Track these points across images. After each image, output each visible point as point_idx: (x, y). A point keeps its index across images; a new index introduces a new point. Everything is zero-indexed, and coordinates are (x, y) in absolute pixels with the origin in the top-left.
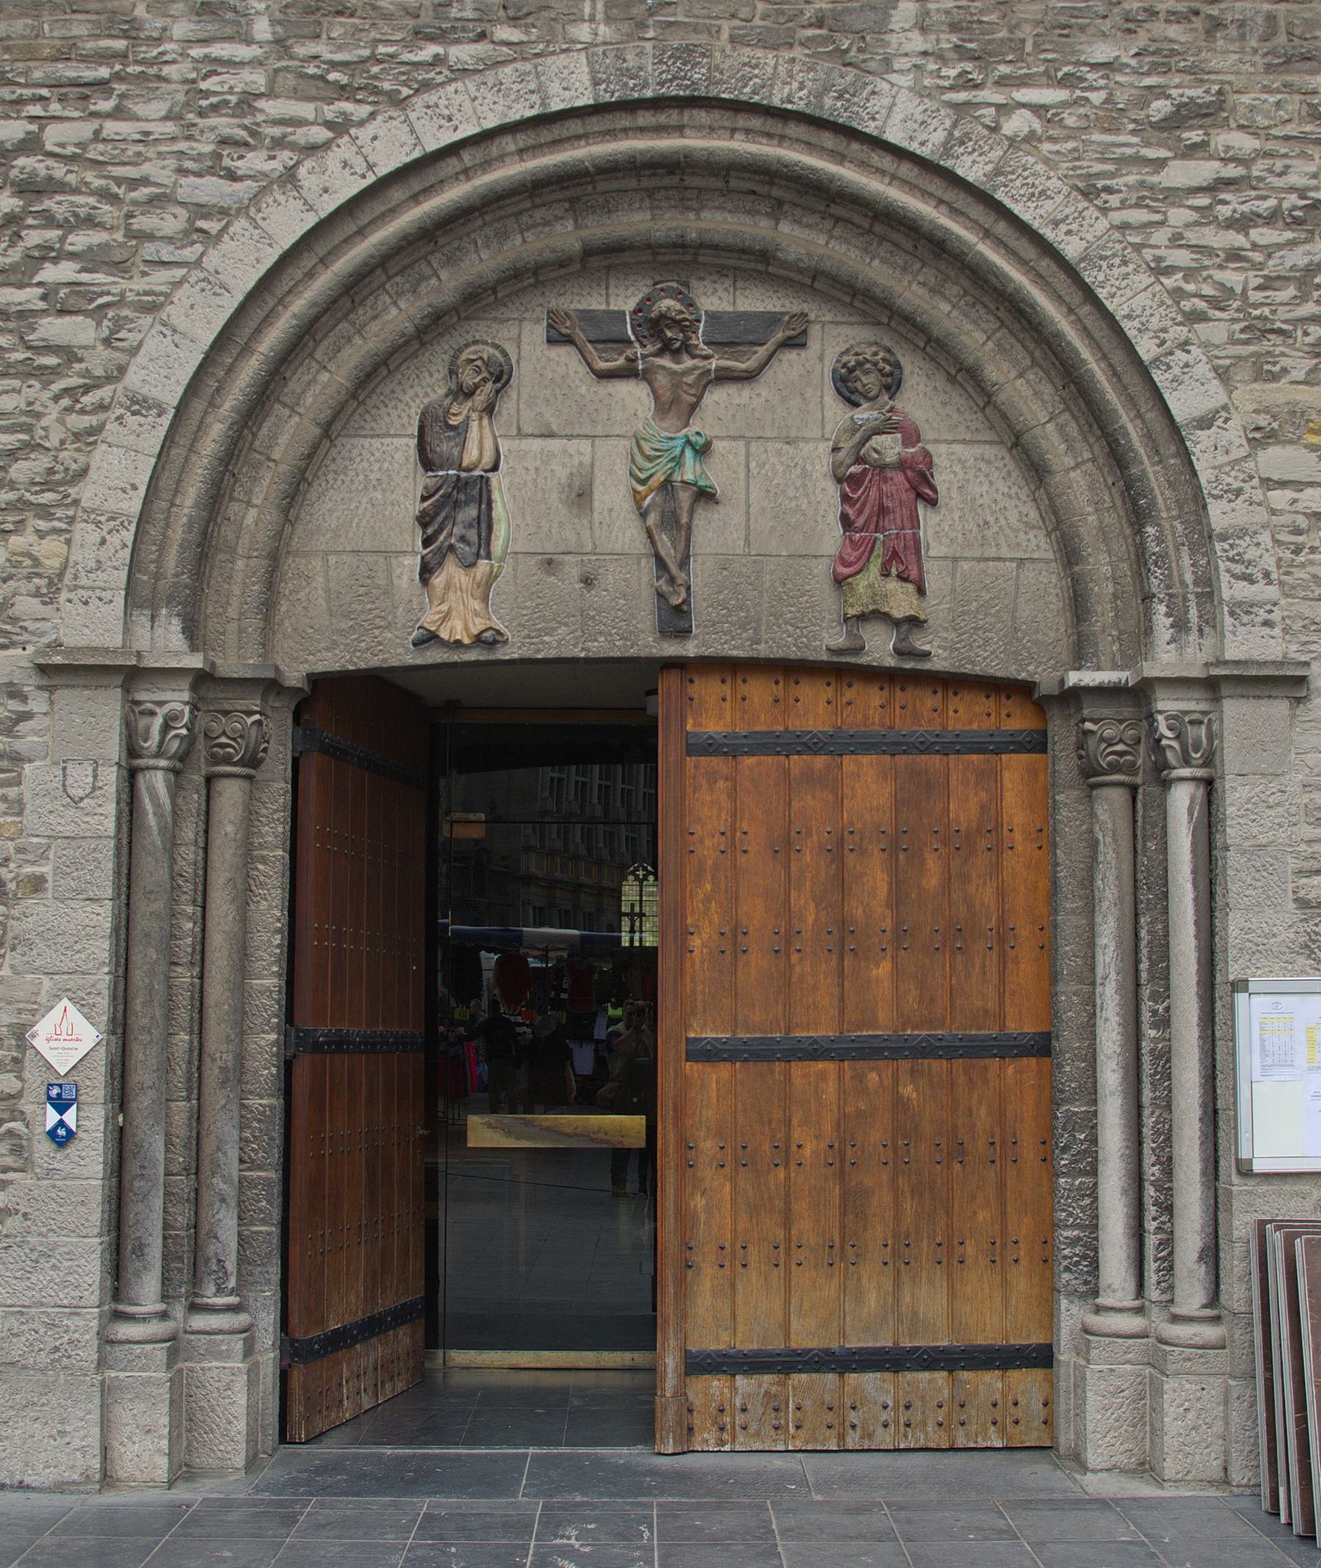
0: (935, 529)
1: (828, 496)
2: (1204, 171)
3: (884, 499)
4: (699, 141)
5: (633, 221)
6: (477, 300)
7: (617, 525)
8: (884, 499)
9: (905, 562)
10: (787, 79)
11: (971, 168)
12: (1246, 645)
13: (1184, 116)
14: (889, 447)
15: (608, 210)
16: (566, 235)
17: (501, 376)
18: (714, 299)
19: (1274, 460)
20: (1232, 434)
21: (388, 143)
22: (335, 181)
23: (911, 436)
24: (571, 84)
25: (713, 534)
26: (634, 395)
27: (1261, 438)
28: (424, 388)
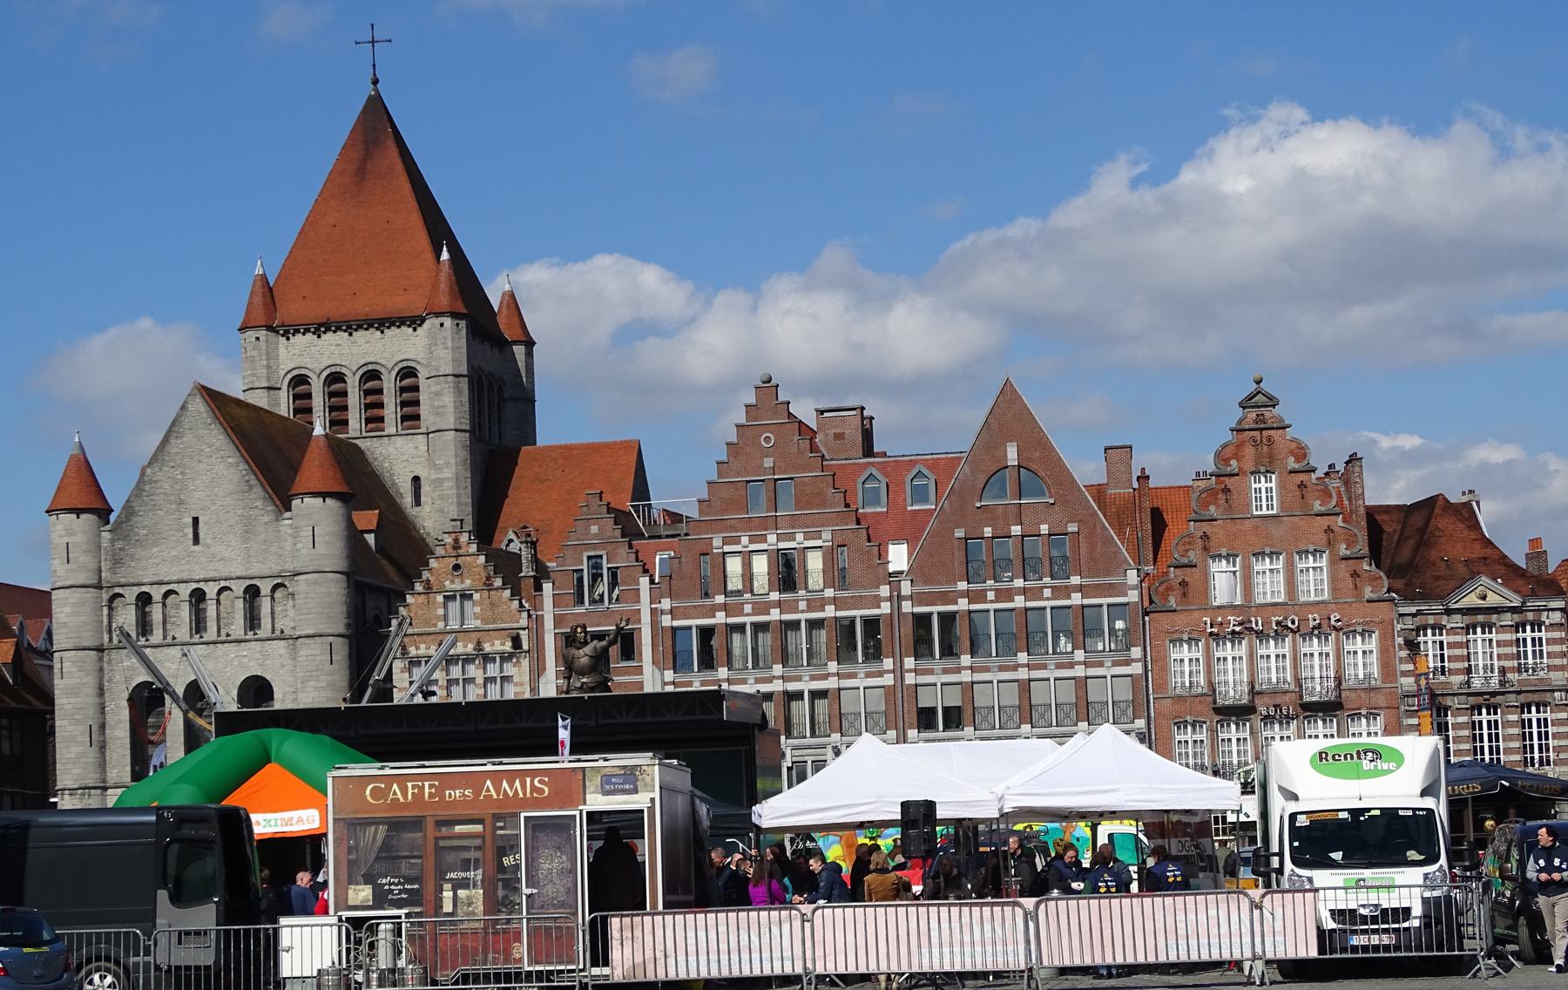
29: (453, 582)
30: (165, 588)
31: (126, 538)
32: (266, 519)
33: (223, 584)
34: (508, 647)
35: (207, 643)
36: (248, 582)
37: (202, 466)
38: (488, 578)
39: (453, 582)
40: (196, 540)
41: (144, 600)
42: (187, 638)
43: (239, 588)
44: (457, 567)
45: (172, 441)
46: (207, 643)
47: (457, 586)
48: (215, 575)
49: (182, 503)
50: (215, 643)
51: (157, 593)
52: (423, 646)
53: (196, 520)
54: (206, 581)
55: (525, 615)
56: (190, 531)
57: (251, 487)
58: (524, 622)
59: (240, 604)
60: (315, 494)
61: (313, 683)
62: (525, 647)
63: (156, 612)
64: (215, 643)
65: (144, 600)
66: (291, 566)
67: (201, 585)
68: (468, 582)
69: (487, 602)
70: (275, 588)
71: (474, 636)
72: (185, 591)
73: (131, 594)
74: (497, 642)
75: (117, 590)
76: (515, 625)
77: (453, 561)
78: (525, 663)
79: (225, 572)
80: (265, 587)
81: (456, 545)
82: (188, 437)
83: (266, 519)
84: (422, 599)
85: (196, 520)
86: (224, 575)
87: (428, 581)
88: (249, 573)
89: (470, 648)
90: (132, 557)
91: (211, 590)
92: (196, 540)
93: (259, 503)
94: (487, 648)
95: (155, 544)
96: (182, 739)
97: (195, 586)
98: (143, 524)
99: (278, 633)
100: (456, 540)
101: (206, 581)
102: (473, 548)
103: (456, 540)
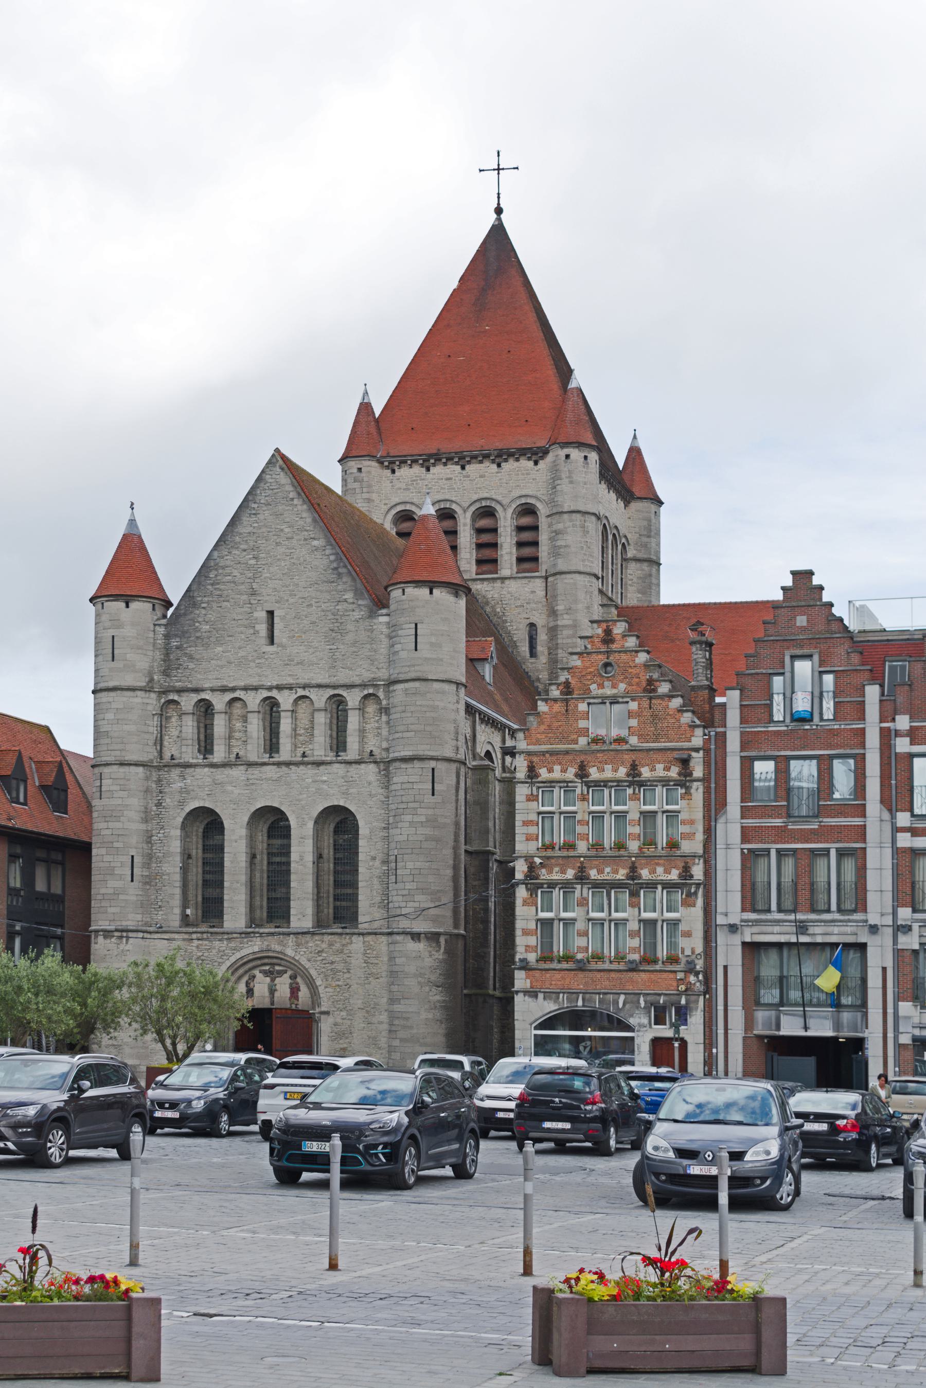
0: (300, 994)
1: (288, 991)
2: (321, 958)
3: (294, 990)
4: (271, 954)
5: (266, 961)
6: (250, 969)
7: (267, 994)
8: (294, 990)
9: (297, 998)
10: (278, 948)
11: (297, 958)
12: (323, 1009)
13: (319, 952)
14: (294, 985)
15: (515, 645)
16: (259, 962)
17: (254, 977)
18: (277, 968)
19: (327, 990)
20: (323, 987)
21: (238, 955)
22: (233, 959)
23: (297, 984)
24: (256, 949)
25: (277, 994)
26: (268, 979)
27: (326, 987)
28: (246, 978)
29: (601, 686)
30: (229, 696)
31: (183, 634)
32: (357, 615)
33: (301, 692)
34: (674, 773)
35: (279, 764)
36: (332, 692)
37: (281, 550)
38: (650, 682)
39: (601, 686)
40: (271, 640)
41: (205, 710)
42: (253, 757)
43: (320, 698)
44: (607, 665)
45: (245, 519)
46: (279, 764)
47: (609, 691)
48: (290, 680)
49: (254, 593)
50: (288, 764)
51: (219, 702)
52: (557, 768)
53: (271, 613)
54: (279, 688)
55: (699, 732)
56: (263, 629)
57: (340, 575)
58: (697, 740)
59: (321, 719)
60: (418, 583)
61: (408, 818)
62: (698, 772)
63: (219, 725)
64: (288, 764)
65: (205, 710)
66: (383, 674)
67: (274, 693)
68: (622, 686)
69: (647, 713)
70: (366, 697)
71: (628, 758)
72: (254, 700)
73: (188, 702)
74: (660, 767)
75: (172, 696)
76: (686, 745)
77: (602, 659)
78: (698, 792)
79: (305, 677)
80: (353, 698)
81: (608, 638)
82: (265, 514)
83: (357, 615)
84: (558, 707)
85: (271, 613)
86: (302, 681)
87: (567, 684)
88: (333, 680)
89: (622, 772)
90: (191, 657)
91: (285, 700)
92: (271, 640)
93: (349, 596)
94: (646, 773)
95: (219, 642)
96: (243, 878)
97: (266, 694)
98: (205, 619)
99: (366, 755)
100: (608, 632)
101: (279, 688)
102: (632, 642)
103: (608, 632)
